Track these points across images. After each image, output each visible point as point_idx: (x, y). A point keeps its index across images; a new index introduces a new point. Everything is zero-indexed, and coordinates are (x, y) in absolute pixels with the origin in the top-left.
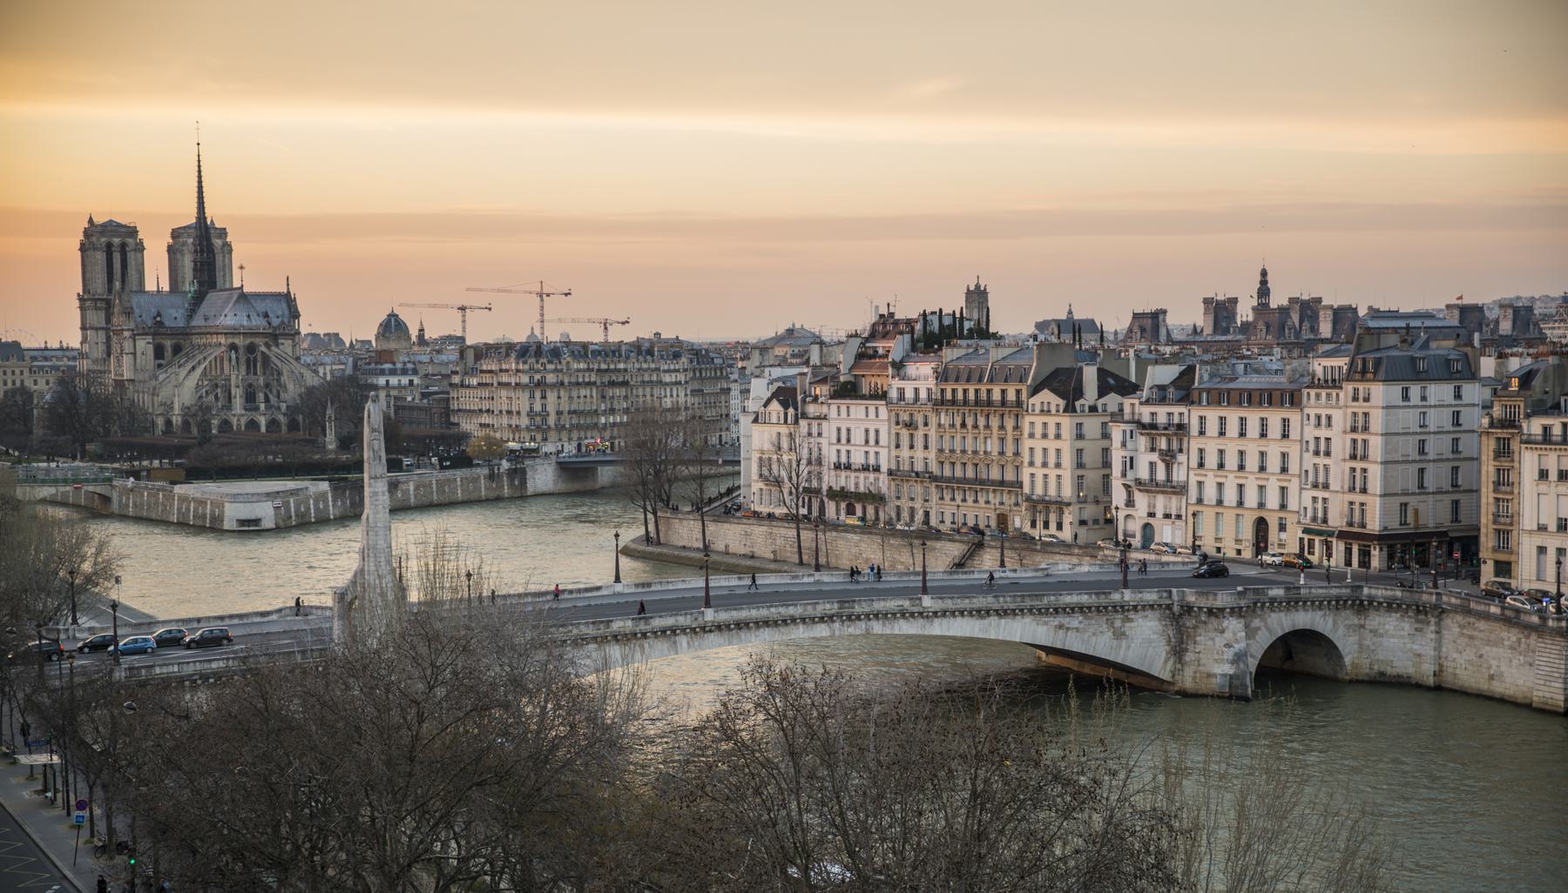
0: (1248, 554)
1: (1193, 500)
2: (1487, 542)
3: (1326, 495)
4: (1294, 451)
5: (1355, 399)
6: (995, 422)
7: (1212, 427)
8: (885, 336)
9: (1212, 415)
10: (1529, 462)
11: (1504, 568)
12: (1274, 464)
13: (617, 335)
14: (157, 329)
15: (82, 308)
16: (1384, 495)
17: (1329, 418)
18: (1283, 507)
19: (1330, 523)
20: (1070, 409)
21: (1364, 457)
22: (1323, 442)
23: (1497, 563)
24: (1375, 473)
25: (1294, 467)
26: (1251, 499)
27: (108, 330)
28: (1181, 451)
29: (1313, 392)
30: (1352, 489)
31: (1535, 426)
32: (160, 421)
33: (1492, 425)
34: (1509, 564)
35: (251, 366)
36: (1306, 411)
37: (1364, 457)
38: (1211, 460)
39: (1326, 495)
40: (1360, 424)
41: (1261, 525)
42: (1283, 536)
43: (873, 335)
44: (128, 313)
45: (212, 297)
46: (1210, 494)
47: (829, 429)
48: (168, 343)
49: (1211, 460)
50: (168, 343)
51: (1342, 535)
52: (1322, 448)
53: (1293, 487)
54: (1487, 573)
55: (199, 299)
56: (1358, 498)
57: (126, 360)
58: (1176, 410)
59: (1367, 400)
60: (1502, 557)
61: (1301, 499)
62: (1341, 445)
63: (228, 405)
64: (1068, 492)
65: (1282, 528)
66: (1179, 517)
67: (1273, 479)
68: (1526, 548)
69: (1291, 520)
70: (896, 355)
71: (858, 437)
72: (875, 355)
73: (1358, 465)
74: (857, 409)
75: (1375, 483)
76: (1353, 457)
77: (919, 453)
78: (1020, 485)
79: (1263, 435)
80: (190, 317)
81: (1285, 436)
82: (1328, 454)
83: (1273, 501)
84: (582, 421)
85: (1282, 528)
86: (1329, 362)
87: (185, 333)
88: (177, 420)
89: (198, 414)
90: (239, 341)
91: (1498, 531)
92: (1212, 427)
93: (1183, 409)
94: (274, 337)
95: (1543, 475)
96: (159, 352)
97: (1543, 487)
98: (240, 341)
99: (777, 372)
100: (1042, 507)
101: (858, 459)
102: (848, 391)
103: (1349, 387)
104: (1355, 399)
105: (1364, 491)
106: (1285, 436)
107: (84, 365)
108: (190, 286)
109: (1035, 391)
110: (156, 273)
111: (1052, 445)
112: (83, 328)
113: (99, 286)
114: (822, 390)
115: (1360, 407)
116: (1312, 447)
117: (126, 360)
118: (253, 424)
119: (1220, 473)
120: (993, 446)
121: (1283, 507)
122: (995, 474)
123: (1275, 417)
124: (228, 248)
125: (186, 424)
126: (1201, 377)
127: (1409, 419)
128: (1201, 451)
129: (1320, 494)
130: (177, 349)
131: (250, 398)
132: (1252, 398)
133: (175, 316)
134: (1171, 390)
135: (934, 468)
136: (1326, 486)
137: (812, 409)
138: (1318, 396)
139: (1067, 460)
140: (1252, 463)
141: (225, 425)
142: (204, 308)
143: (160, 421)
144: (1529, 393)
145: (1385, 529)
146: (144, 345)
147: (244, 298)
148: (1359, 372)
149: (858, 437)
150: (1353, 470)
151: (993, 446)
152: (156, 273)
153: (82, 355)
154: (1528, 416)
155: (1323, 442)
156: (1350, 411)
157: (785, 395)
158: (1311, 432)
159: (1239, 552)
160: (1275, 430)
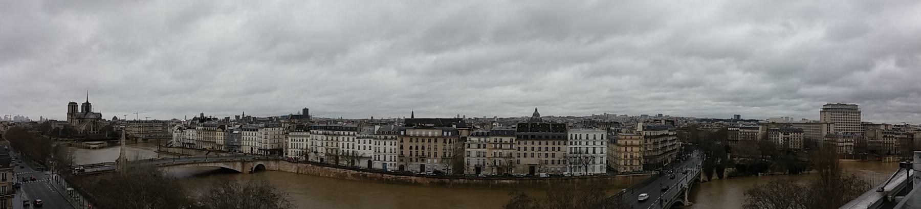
0: (250, 153)
2: (284, 150)
4: (257, 138)
6: (212, 133)
8: (195, 120)
9: (245, 132)
10: (290, 139)
11: (286, 154)
12: (254, 139)
13: (148, 119)
14: (79, 118)
15: (68, 115)
20: (223, 131)
25: (257, 140)
26: (250, 145)
27: (72, 119)
31: (290, 134)
32: (79, 132)
35: (94, 124)
41: (252, 149)
43: (193, 120)
44: (75, 115)
45: (88, 113)
47: (187, 134)
48: (81, 120)
50: (81, 120)
51: (264, 150)
53: (257, 143)
54: (284, 154)
55: (86, 113)
57: (74, 123)
61: (258, 145)
62: (263, 137)
63: (90, 130)
64: (223, 143)
70: (197, 123)
71: (191, 135)
72: (193, 123)
74: (191, 131)
77: (200, 137)
78: (215, 142)
80: (85, 116)
81: (255, 135)
83: (254, 145)
84: (146, 132)
87: (84, 119)
88: (82, 132)
89: (85, 131)
90: (93, 120)
94: (98, 119)
95: (292, 140)
96: (80, 122)
98: (93, 120)
99: (178, 125)
100: (219, 145)
101: (191, 138)
102: (189, 128)
106: (255, 135)
107: (68, 123)
108: (85, 112)
109: (218, 128)
110: (80, 110)
111: (220, 136)
112: (68, 118)
113: (71, 112)
114: (186, 128)
117: (74, 123)
118: (94, 133)
120: (212, 137)
122: (212, 141)
123: (254, 133)
124: (91, 106)
125: (83, 133)
130: (82, 121)
131: (93, 128)
132: (251, 130)
133: (82, 117)
135: (203, 140)
137: (184, 131)
139: (223, 139)
140: (251, 139)
141: (90, 133)
142: (87, 115)
143: (79, 132)
146: (77, 120)
147: (93, 113)
148: (266, 126)
149: (191, 135)
151: (212, 137)
152: (80, 110)
153: (67, 122)
157: (180, 129)
158: (259, 135)
160: (254, 135)
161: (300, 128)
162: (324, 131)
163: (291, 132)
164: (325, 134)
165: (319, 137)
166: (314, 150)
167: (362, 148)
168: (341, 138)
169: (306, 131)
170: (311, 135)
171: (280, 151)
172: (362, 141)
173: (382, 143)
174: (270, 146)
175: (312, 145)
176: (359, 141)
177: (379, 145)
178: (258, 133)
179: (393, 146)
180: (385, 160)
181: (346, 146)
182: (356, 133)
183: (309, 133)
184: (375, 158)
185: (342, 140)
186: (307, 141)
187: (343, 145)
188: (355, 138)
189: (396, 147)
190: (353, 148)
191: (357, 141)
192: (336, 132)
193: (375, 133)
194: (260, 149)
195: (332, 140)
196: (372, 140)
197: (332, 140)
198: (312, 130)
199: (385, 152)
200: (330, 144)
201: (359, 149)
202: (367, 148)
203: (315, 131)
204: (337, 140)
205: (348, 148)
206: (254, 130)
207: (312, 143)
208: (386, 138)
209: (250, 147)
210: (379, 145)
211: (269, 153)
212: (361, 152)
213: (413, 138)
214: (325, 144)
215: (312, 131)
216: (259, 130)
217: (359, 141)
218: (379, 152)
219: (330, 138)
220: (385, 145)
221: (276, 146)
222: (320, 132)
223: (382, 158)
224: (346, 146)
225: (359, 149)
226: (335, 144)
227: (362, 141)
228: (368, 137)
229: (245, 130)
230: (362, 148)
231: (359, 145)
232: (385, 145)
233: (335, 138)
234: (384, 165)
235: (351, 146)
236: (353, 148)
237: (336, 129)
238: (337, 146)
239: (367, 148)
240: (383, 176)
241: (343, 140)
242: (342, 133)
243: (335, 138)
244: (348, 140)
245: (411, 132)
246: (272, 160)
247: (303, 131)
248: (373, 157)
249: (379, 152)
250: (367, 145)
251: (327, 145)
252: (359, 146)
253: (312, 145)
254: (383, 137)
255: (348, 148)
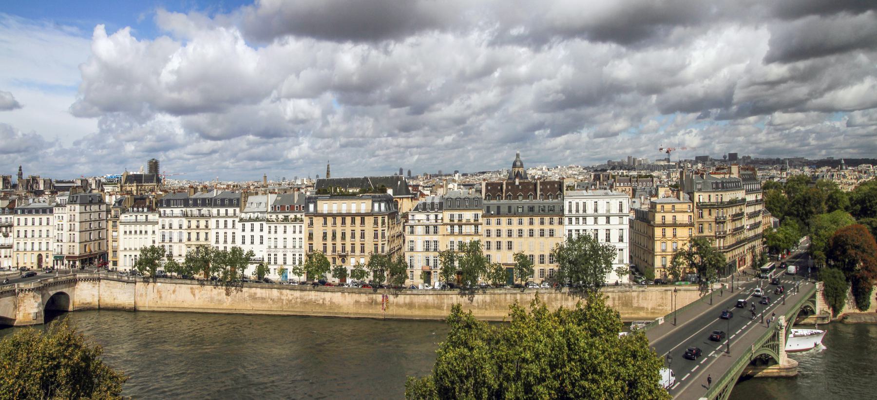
1: (16, 250)
2: (110, 255)
3: (62, 244)
4: (50, 228)
5: (71, 210)
7: (22, 222)
9: (22, 218)
10: (121, 228)
11: (115, 263)
12: (44, 234)
16: (80, 243)
17: (62, 217)
18: (47, 249)
19: (63, 253)
21: (74, 230)
22: (60, 225)
23: (113, 261)
24: (77, 234)
25: (51, 235)
26: (36, 248)
28: (11, 232)
29: (57, 208)
30: (70, 241)
31: (123, 217)
33: (111, 218)
34: (116, 261)
36: (55, 215)
37: (74, 230)
38: (22, 234)
39: (62, 244)
40: (73, 219)
41: (40, 256)
42: (47, 260)
46: (22, 247)
49: (22, 234)
51: (67, 257)
52: (60, 228)
53: (51, 242)
54: (110, 266)
56: (72, 244)
58: (9, 217)
59: (74, 210)
60: (115, 260)
62: (66, 227)
65: (47, 257)
66: (10, 256)
67: (44, 240)
68: (121, 255)
69: (50, 254)
73: (72, 233)
75: (77, 240)
76: (70, 230)
79: (40, 224)
81: (48, 224)
82: (62, 230)
83: (44, 248)
85: (47, 257)
86: (62, 198)
91: (113, 251)
92: (22, 222)
93: (12, 216)
95: (125, 232)
97: (125, 236)
103: (68, 206)
104: (71, 210)
105: (74, 242)
106: (48, 224)
115: (72, 213)
116: (57, 227)
119: (26, 239)
121: (47, 249)
123: (44, 218)
126: (18, 204)
127: (86, 217)
128: (18, 231)
129: (60, 244)
132: (37, 211)
134: (7, 209)
136: (62, 241)
138: (59, 209)
140: (37, 234)
144: (121, 207)
145: (80, 254)
148: (72, 202)
150: (70, 234)
154: (121, 214)
155: (60, 225)
156: (69, 214)
159: (32, 267)
161: (139, 202)
162: (184, 209)
163: (124, 211)
164: (185, 215)
165: (176, 222)
166: (167, 253)
167: (248, 240)
168: (212, 223)
169: (151, 209)
170: (160, 220)
171: (103, 256)
172: (248, 225)
173: (280, 228)
174: (80, 248)
175: (163, 241)
176: (244, 225)
177: (276, 232)
178: (54, 219)
179: (297, 235)
180: (285, 263)
181: (221, 239)
182: (238, 210)
183: (157, 215)
184: (269, 259)
185: (215, 227)
186: (154, 232)
187: (217, 237)
188: (237, 220)
189: (302, 236)
190: (233, 241)
191: (239, 225)
192: (205, 211)
193: (269, 211)
194: (58, 258)
195: (198, 227)
196: (264, 223)
197: (198, 227)
198: (162, 206)
199: (285, 247)
200: (194, 236)
201: (243, 243)
202: (257, 240)
203: (168, 211)
204: (207, 227)
205: (225, 242)
206: (44, 211)
207: (164, 236)
208: (286, 219)
209: (36, 254)
210: (276, 232)
211: (78, 263)
212: (246, 249)
213: (356, 218)
214: (185, 237)
215: (162, 210)
216: (56, 210)
217: (244, 225)
218: (276, 247)
219: (194, 223)
220: (285, 232)
221: (93, 248)
222: (177, 211)
223: (280, 261)
224: (221, 239)
225: (243, 243)
226: (202, 236)
227: (248, 225)
228: (257, 219)
229: (23, 212)
230: (248, 240)
231: (252, 233)
232: (285, 232)
233: (202, 223)
234: (283, 272)
235: (230, 239)
236: (233, 241)
237: (205, 203)
238: (206, 239)
239: (257, 240)
240: (281, 293)
241: (218, 227)
242: (214, 211)
243: (202, 223)
244: (226, 226)
245: (325, 206)
246: (86, 280)
247: (145, 210)
248: (266, 260)
249: (276, 247)
250: (257, 233)
251: (189, 240)
252: (244, 237)
253: (163, 241)
254: (281, 216)
255: (225, 242)
